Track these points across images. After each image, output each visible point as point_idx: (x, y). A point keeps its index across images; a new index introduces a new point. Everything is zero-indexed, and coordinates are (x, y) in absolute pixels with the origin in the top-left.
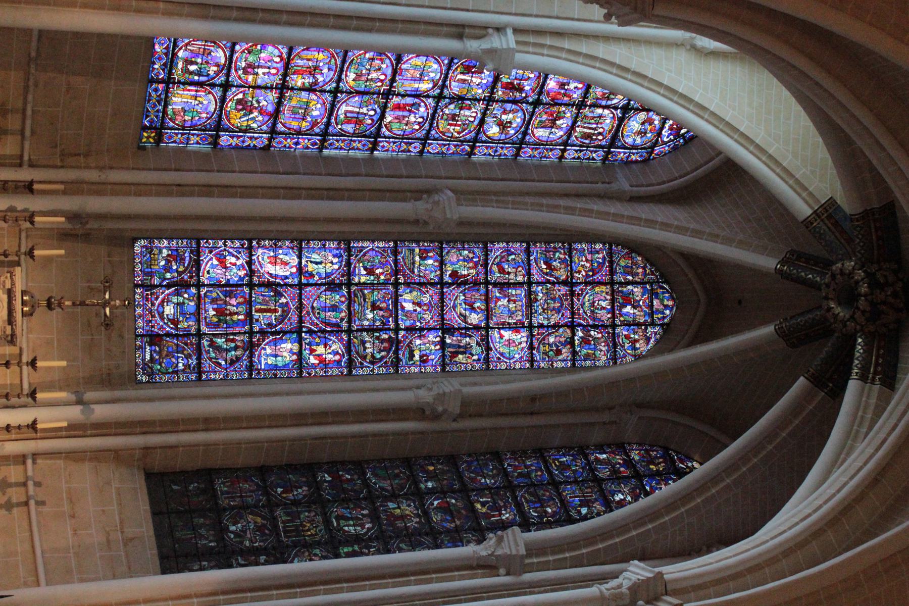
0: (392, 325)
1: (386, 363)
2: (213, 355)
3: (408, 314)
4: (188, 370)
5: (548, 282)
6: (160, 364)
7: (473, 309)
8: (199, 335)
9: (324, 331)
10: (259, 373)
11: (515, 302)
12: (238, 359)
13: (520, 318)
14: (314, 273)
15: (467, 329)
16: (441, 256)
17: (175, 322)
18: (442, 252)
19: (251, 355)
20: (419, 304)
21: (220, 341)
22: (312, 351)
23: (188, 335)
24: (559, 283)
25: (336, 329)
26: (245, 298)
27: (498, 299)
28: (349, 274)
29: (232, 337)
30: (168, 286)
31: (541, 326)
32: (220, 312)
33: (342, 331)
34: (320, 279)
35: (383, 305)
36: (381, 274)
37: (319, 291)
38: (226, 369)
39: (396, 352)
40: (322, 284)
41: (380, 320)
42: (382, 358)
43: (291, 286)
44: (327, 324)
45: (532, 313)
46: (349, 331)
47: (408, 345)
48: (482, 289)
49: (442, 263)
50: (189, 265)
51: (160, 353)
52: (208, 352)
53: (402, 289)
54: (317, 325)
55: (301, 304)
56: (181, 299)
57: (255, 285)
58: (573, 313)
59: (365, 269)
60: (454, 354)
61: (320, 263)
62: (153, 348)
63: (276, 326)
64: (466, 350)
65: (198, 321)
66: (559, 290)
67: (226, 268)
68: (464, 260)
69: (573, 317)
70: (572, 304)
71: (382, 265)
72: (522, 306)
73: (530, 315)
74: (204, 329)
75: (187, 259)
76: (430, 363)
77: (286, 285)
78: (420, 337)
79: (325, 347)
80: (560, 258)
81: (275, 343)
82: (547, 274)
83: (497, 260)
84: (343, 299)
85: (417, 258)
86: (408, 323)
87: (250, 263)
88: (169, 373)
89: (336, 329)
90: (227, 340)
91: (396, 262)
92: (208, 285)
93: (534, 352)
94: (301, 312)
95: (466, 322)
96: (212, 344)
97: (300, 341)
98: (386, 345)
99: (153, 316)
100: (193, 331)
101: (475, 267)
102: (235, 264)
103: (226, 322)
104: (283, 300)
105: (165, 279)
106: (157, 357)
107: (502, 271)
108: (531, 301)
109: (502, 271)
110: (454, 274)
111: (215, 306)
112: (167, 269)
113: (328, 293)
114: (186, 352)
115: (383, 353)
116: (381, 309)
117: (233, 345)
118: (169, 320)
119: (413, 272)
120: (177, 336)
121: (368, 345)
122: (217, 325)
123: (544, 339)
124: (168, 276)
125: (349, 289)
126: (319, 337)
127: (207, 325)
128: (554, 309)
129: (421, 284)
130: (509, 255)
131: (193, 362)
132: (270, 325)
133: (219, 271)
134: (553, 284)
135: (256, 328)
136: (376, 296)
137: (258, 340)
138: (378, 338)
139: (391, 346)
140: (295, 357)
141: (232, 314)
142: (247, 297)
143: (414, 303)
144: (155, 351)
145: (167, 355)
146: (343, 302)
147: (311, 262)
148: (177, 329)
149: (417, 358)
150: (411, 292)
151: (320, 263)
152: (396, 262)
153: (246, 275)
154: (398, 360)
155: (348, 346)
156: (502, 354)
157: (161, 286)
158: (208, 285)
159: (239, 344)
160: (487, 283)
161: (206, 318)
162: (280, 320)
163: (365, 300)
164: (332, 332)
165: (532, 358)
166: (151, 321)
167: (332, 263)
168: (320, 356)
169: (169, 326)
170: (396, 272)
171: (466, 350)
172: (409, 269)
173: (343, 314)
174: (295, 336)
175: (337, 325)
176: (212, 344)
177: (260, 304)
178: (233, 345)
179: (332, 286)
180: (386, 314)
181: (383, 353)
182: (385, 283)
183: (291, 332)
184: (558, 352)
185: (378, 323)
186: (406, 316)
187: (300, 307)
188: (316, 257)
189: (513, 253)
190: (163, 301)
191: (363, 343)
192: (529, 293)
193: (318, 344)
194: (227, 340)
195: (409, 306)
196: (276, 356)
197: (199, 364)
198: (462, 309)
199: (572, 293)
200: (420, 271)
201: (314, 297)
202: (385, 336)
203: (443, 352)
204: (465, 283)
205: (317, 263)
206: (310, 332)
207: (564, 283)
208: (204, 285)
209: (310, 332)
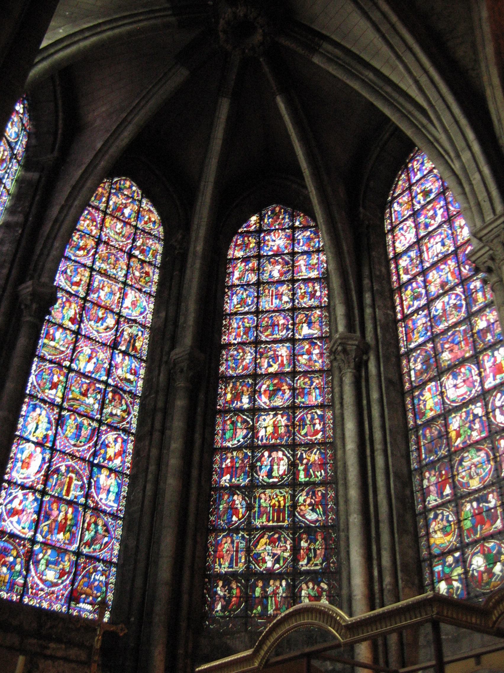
0: (102, 386)
1: (131, 403)
2: (98, 547)
3: (97, 369)
4: (107, 573)
5: (94, 255)
6: (98, 597)
7: (103, 319)
8: (78, 554)
9: (96, 445)
10: (121, 511)
11: (103, 286)
12: (105, 525)
13: (117, 288)
14: (45, 433)
15: (117, 330)
16: (55, 324)
17: (63, 573)
18: (52, 322)
19: (104, 512)
20: (90, 358)
21: (88, 536)
22: (110, 459)
23: (76, 564)
24: (97, 248)
25: (96, 432)
26: (54, 502)
27: (99, 297)
28: (52, 404)
29: (86, 525)
30: (28, 570)
31: (126, 276)
32: (62, 528)
33: (99, 429)
34: (51, 430)
35: (85, 386)
36: (58, 378)
37: (62, 435)
38: (112, 538)
39: (125, 392)
40: (56, 429)
41: (96, 395)
42: (126, 404)
43: (52, 457)
44: (91, 439)
45: (115, 278)
46: (100, 422)
47: (121, 380)
48: (88, 305)
49: (61, 326)
50: (12, 545)
51: (88, 595)
52: (95, 550)
53: (74, 366)
54: (89, 447)
55: (69, 454)
56: (43, 562)
57: (44, 488)
58: (121, 250)
59: (51, 389)
60: (134, 348)
61: (37, 425)
62: (82, 600)
63: (84, 482)
64: (133, 338)
65: (66, 551)
66: (102, 251)
67: (23, 511)
68: (63, 308)
69: (124, 252)
70: (114, 247)
71: (51, 374)
72: (108, 283)
73: (115, 280)
74: (74, 547)
75: (6, 544)
76: (137, 369)
77: (50, 461)
78: (117, 368)
79: (109, 447)
80: (78, 239)
81: (98, 488)
82: (88, 253)
83: (69, 283)
84: (73, 417)
85: (52, 343)
86: (103, 372)
87: (23, 487)
88: (106, 590)
89: (96, 432)
90: (88, 529)
91: (51, 362)
92: (36, 532)
93: (144, 290)
94: (77, 457)
95: (112, 328)
96: (89, 544)
97: (100, 467)
98: (117, 397)
99: (53, 593)
100: (74, 558)
101: (70, 303)
102: (21, 502)
103: (72, 526)
104: (63, 469)
105: (20, 572)
106: (91, 598)
107: (78, 284)
108: (105, 274)
109: (78, 284)
110: (72, 320)
111: (56, 531)
112: (11, 567)
113: (64, 428)
114: (91, 571)
115: (123, 402)
116: (87, 390)
117: (93, 526)
118: (60, 578)
119: (63, 352)
120: (75, 575)
121: (114, 412)
122: (73, 535)
123: (136, 279)
124: (18, 567)
125: (65, 409)
126: (100, 449)
127: (71, 543)
128: (116, 261)
129: (74, 350)
130: (66, 273)
131: (101, 567)
132: (82, 487)
133: (25, 518)
134: (96, 253)
135: (82, 500)
136: (76, 390)
137: (93, 502)
138: (110, 402)
139: (119, 393)
140: (113, 475)
141: (66, 518)
142: (53, 499)
143: (89, 362)
144: (85, 599)
145: (91, 589)
146: (75, 419)
147: (34, 432)
148: (69, 573)
149: (132, 377)
150: (79, 360)
151: (37, 425)
152: (51, 362)
153: (34, 493)
154: (130, 392)
155: (113, 428)
156: (141, 314)
157: (25, 577)
158: (36, 532)
159: (93, 520)
160: (85, 299)
161: (64, 543)
162: (80, 477)
163: (78, 400)
164: (98, 437)
165: (147, 293)
166: (57, 597)
167: (40, 415)
168: (115, 454)
169: (66, 580)
170: (60, 365)
171: (133, 338)
172: (60, 354)
173: (85, 422)
174: (95, 469)
175: (94, 430)
176: (89, 544)
177: (62, 490)
178: (93, 526)
179: (60, 422)
180: (93, 388)
181: (123, 402)
182: (67, 376)
183: (91, 471)
184: (147, 274)
185: (99, 397)
186: (98, 372)
187: (73, 456)
188: (31, 427)
189: (66, 269)
190: (41, 579)
191: (111, 415)
192: (99, 272)
193: (106, 453)
194: (88, 529)
195: (90, 367)
196: (109, 491)
197: (104, 561)
198: (100, 329)
199: (107, 243)
200: (64, 346)
201: (66, 441)
202: (110, 395)
203: (132, 356)
204: (81, 316)
205: (37, 428)
206: (95, 455)
207: (98, 244)
208: (34, 536)
209: (95, 455)
